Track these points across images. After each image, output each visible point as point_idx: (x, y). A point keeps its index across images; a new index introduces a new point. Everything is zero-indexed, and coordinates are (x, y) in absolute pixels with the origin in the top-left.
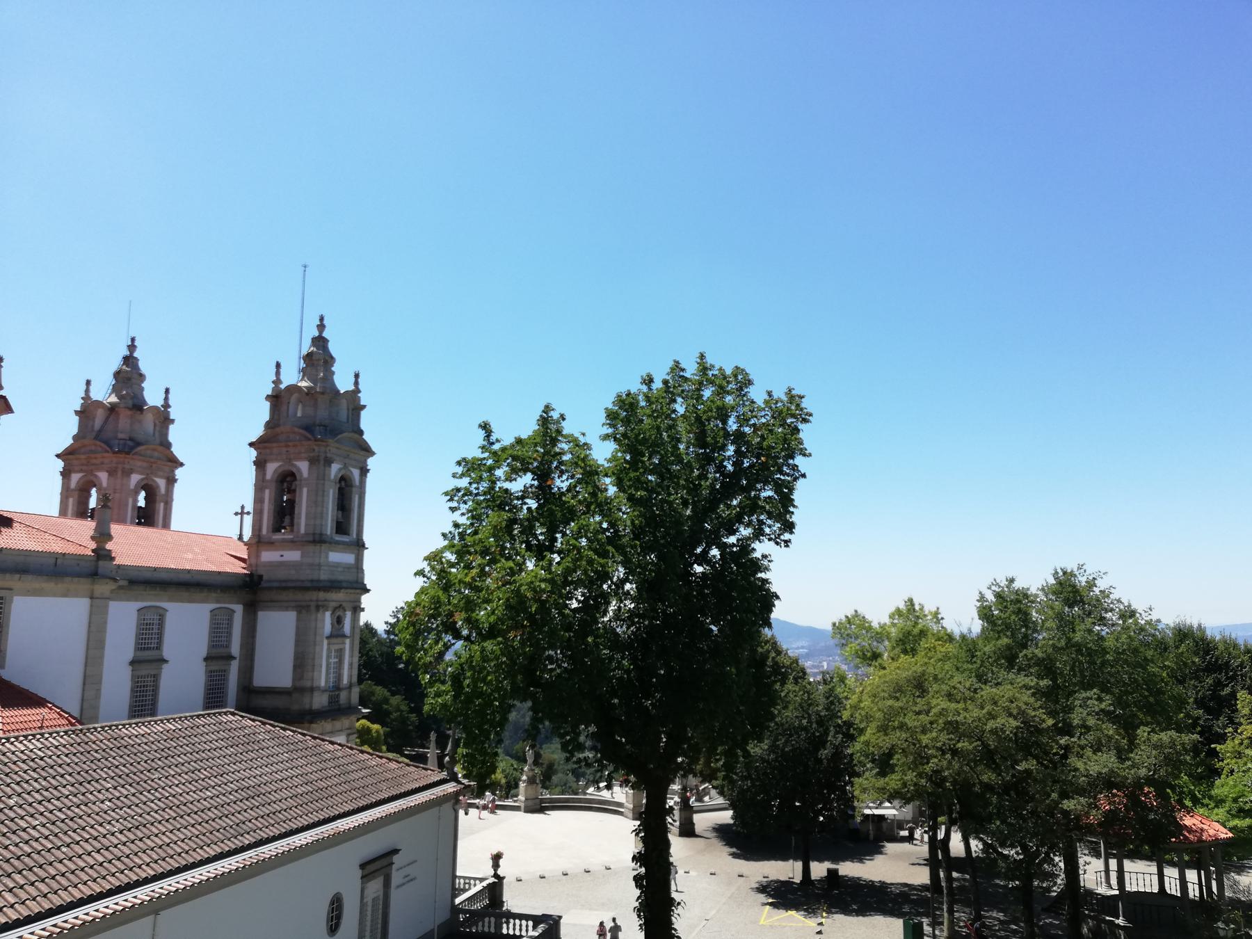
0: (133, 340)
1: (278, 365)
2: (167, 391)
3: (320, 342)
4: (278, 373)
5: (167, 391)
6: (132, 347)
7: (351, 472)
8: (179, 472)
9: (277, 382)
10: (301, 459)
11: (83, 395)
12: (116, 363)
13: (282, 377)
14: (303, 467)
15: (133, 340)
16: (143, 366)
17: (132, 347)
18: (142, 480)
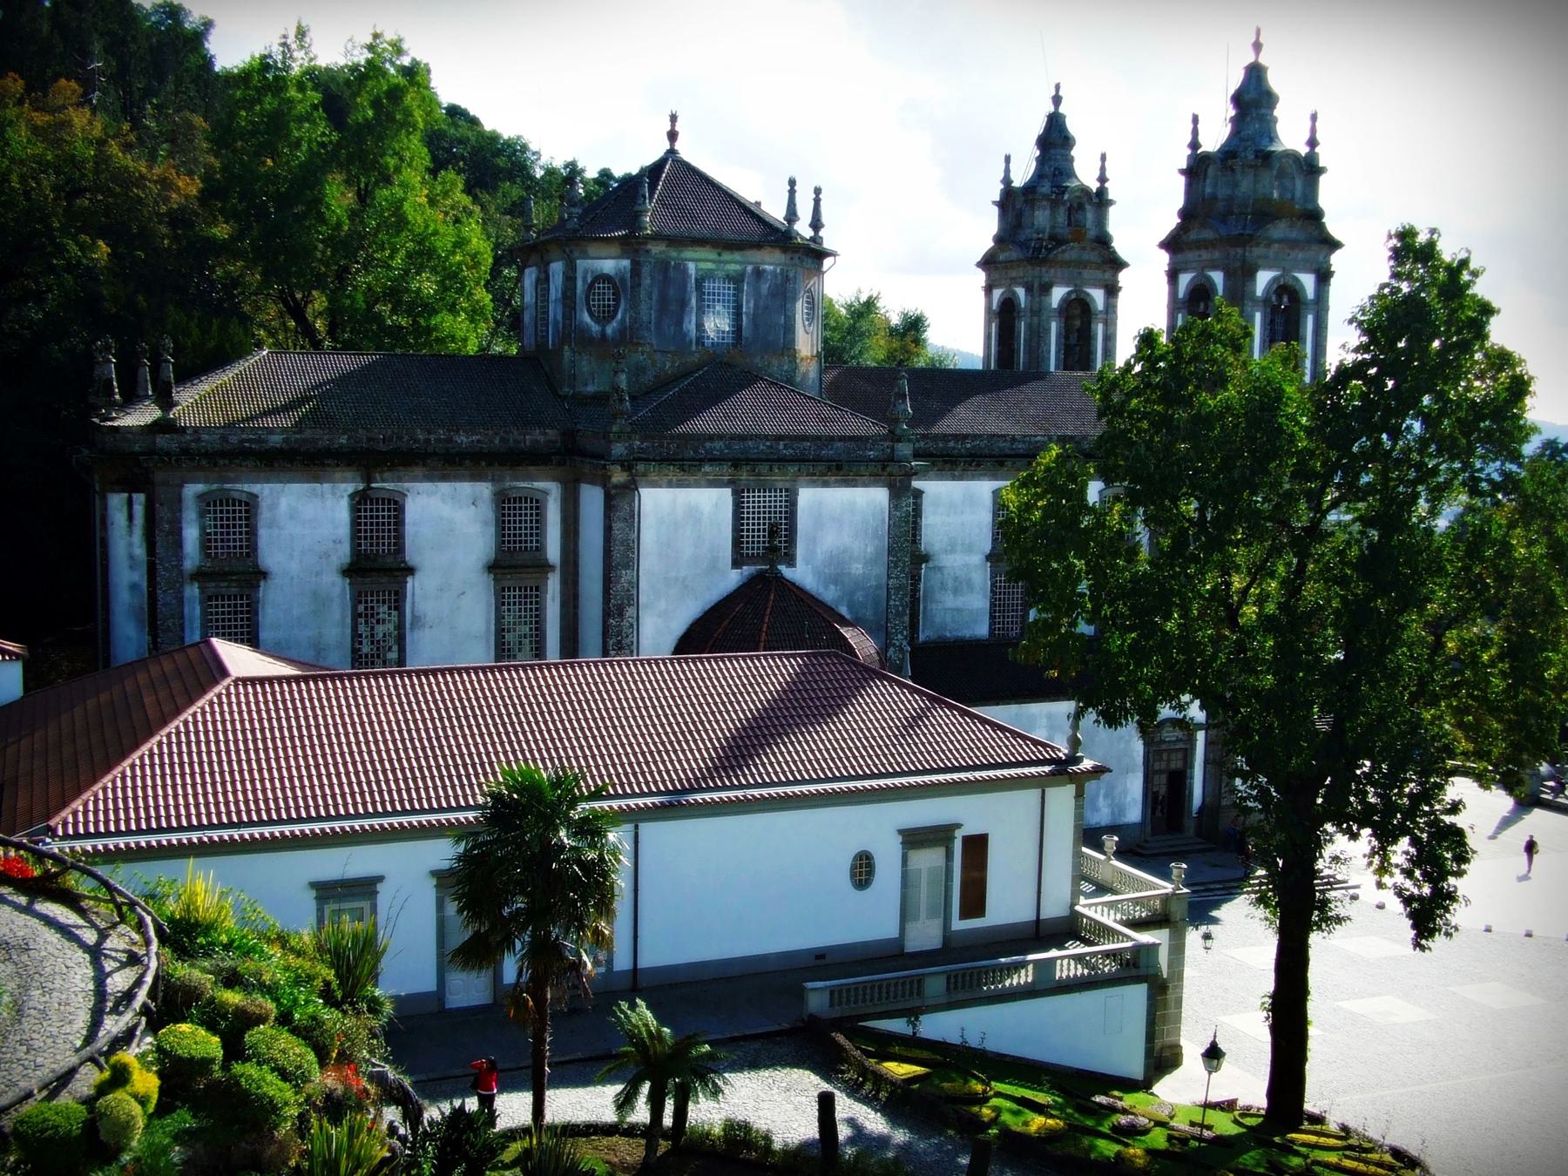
0: (1058, 87)
1: (1195, 120)
2: (1103, 158)
3: (1255, 74)
4: (1195, 132)
5: (1103, 158)
6: (1057, 100)
7: (1297, 279)
8: (1123, 277)
9: (1194, 145)
10: (1215, 268)
11: (1002, 175)
12: (1038, 127)
13: (1201, 139)
14: (1218, 277)
15: (1058, 87)
16: (1072, 126)
17: (1057, 100)
18: (1069, 293)
